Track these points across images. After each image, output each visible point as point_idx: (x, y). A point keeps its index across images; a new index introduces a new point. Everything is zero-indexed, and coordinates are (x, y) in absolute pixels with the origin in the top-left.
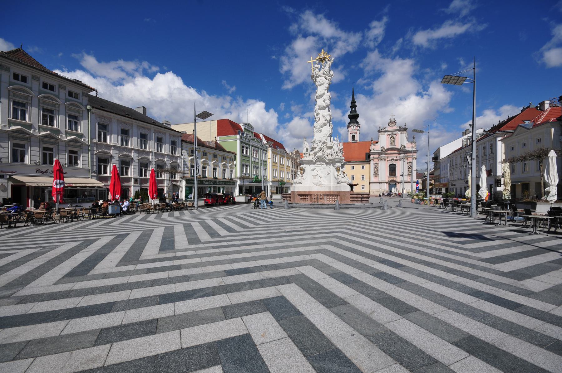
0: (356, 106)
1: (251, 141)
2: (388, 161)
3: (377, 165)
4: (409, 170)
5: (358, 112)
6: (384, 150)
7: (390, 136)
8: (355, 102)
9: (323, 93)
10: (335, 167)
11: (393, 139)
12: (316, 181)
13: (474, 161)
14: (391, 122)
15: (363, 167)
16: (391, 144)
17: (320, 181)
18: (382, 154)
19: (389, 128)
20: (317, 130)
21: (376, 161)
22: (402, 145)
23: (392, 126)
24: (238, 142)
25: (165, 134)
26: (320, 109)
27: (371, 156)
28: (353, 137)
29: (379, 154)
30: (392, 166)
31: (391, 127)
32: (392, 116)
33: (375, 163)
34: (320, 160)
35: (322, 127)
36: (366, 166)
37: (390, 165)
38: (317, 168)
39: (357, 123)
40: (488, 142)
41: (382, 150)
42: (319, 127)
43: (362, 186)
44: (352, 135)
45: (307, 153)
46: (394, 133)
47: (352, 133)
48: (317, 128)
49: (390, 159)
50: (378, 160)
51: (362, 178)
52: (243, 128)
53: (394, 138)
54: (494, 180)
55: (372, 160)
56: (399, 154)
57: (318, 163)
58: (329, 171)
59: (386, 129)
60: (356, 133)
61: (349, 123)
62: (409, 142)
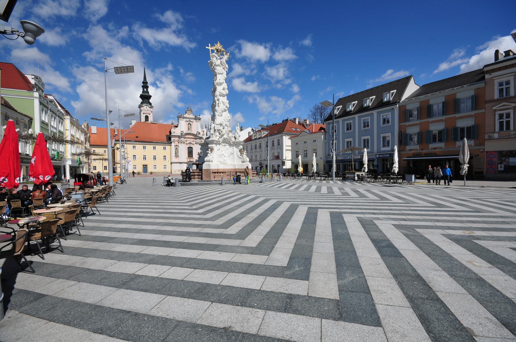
0: (148, 87)
1: (49, 103)
2: (186, 144)
5: (150, 94)
6: (184, 134)
7: (188, 123)
9: (223, 82)
10: (238, 148)
11: (190, 126)
12: (221, 160)
13: (334, 151)
15: (165, 148)
16: (188, 130)
17: (225, 160)
18: (181, 138)
20: (219, 114)
21: (177, 143)
22: (198, 132)
23: (189, 114)
24: (37, 102)
26: (220, 95)
27: (172, 139)
28: (147, 118)
29: (179, 137)
30: (190, 149)
31: (188, 115)
33: (175, 145)
34: (227, 142)
35: (223, 112)
36: (168, 147)
37: (188, 148)
38: (222, 149)
39: (150, 104)
40: (276, 138)
41: (181, 134)
42: (220, 111)
43: (164, 166)
44: (145, 115)
45: (214, 134)
46: (191, 120)
47: (145, 113)
48: (219, 112)
49: (188, 142)
50: (178, 143)
51: (164, 158)
53: (191, 125)
54: (281, 162)
55: (173, 143)
56: (195, 139)
57: (222, 144)
58: (232, 152)
59: (185, 116)
60: (150, 114)
61: (142, 103)
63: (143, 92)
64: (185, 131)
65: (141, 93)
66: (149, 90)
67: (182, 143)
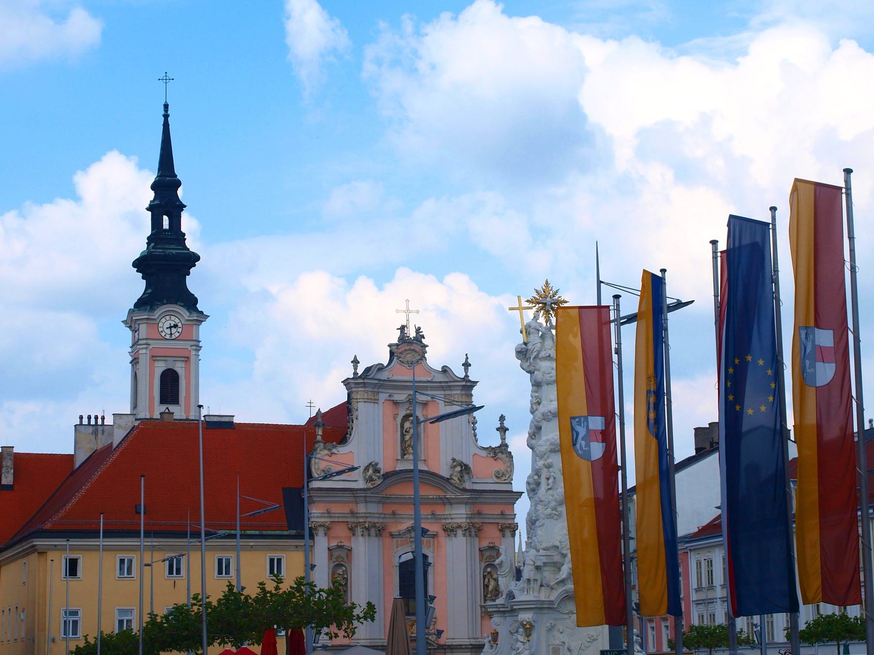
2: (392, 536)
3: (343, 553)
4: (486, 586)
5: (191, 244)
7: (402, 413)
33: (334, 544)
39: (190, 302)
44: (160, 367)
55: (321, 532)
63: (156, 237)
66: (187, 223)
67: (368, 529)
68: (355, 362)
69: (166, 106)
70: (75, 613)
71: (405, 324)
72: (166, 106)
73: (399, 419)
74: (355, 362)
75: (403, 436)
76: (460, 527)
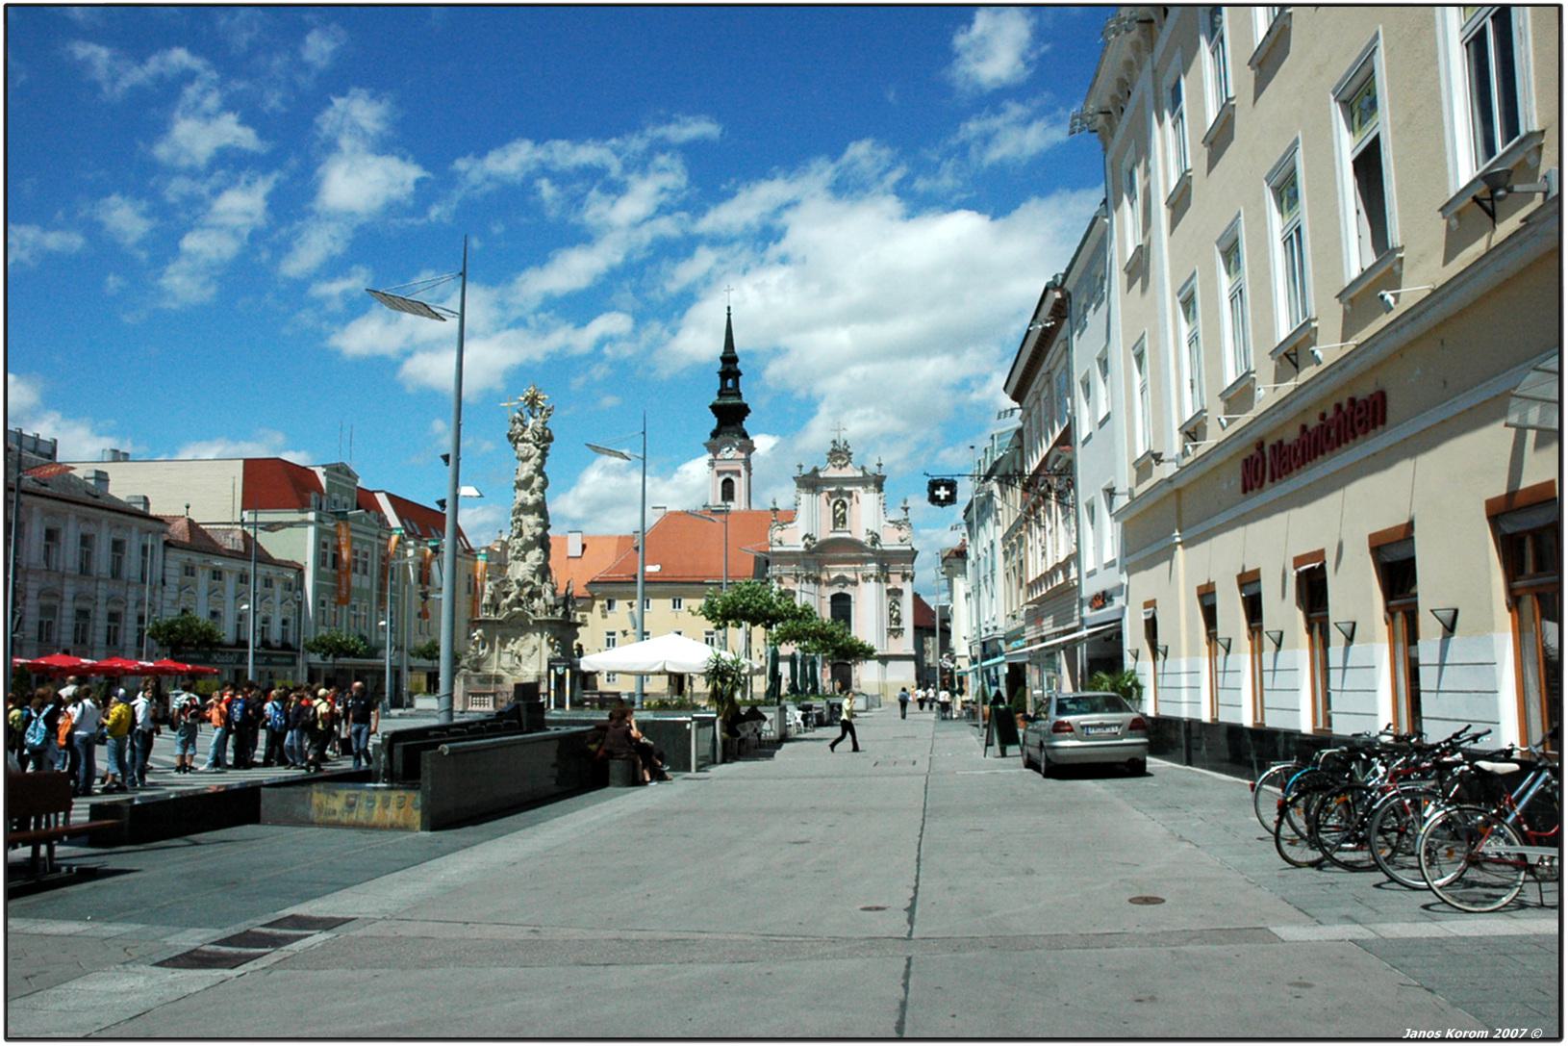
0: (738, 374)
4: (891, 616)
8: (735, 360)
14: (834, 451)
19: (832, 472)
25: (129, 528)
32: (838, 430)
44: (721, 479)
47: (724, 472)
52: (323, 480)
53: (844, 505)
62: (890, 522)
64: (825, 532)
65: (714, 398)
68: (801, 467)
69: (729, 308)
70: (613, 634)
71: (836, 438)
72: (729, 308)
73: (832, 504)
74: (801, 467)
75: (834, 514)
76: (871, 576)
